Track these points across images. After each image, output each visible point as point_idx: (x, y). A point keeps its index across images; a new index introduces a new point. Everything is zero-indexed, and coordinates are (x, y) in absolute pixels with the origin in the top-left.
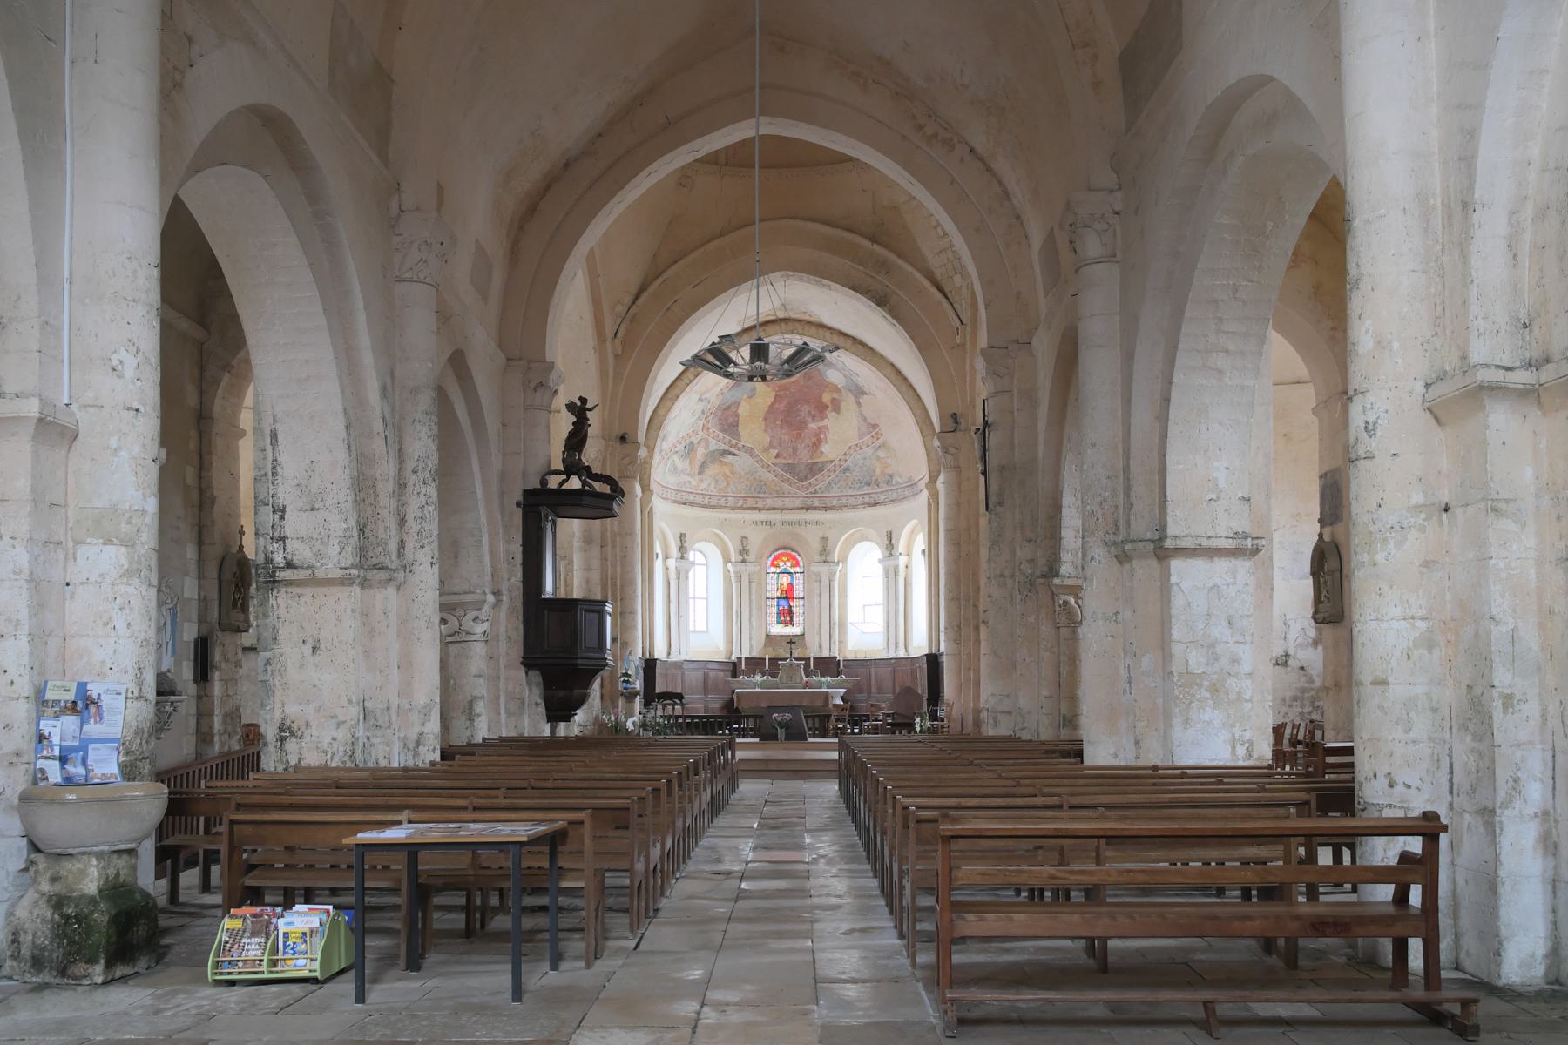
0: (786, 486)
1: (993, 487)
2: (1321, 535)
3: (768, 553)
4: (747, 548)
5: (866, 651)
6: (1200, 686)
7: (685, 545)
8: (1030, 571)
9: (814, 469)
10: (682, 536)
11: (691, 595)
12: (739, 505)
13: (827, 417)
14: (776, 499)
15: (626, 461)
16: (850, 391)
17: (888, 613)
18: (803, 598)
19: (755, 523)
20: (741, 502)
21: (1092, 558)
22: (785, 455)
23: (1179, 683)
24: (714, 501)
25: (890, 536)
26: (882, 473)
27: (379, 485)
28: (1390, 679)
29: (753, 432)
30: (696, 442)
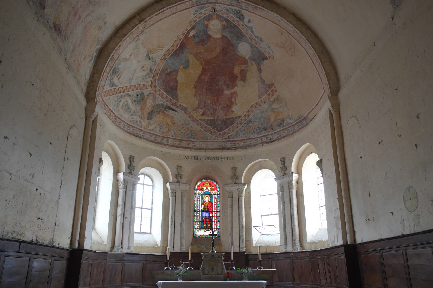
0: (209, 134)
3: (195, 180)
4: (181, 173)
5: (266, 248)
7: (134, 164)
10: (131, 159)
11: (138, 204)
12: (176, 145)
13: (237, 85)
14: (202, 143)
16: (254, 60)
17: (284, 217)
18: (219, 211)
19: (187, 157)
20: (178, 143)
22: (208, 113)
24: (159, 140)
25: (283, 161)
30: (146, 94)
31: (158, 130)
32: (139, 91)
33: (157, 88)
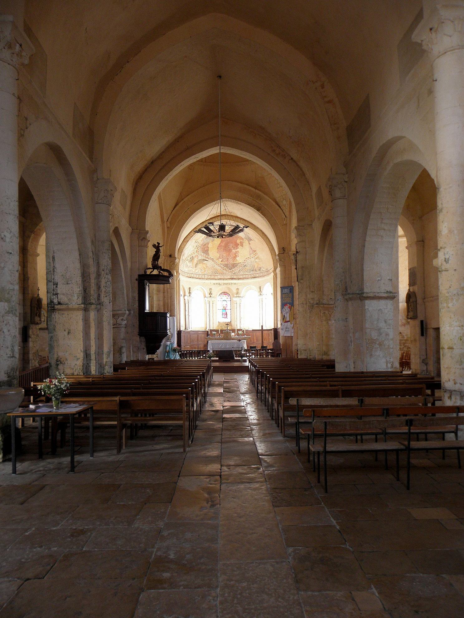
0: (225, 271)
1: (300, 273)
2: (409, 290)
6: (375, 343)
8: (312, 302)
9: (234, 266)
12: (208, 278)
15: (171, 264)
19: (214, 284)
21: (338, 300)
23: (368, 343)
24: (200, 277)
25: (260, 288)
26: (257, 267)
27: (91, 275)
28: (454, 347)
29: (214, 253)
31: (200, 272)
32: (192, 256)
33: (199, 253)
